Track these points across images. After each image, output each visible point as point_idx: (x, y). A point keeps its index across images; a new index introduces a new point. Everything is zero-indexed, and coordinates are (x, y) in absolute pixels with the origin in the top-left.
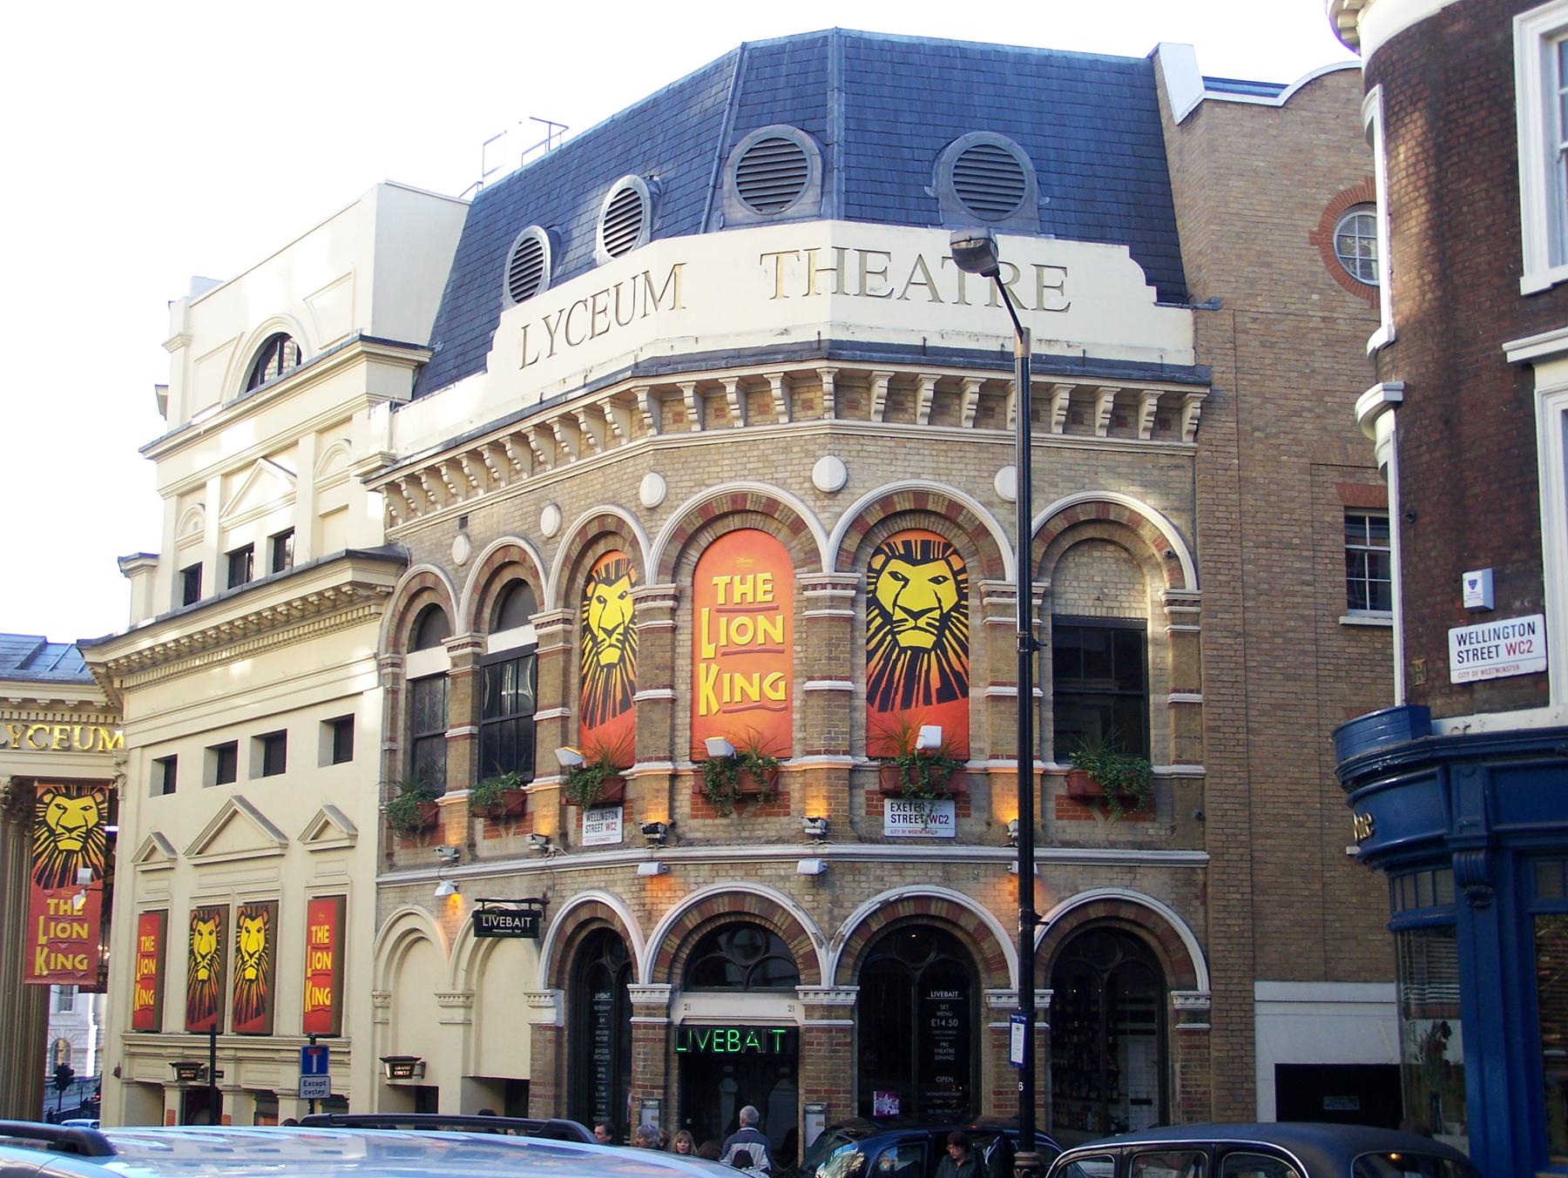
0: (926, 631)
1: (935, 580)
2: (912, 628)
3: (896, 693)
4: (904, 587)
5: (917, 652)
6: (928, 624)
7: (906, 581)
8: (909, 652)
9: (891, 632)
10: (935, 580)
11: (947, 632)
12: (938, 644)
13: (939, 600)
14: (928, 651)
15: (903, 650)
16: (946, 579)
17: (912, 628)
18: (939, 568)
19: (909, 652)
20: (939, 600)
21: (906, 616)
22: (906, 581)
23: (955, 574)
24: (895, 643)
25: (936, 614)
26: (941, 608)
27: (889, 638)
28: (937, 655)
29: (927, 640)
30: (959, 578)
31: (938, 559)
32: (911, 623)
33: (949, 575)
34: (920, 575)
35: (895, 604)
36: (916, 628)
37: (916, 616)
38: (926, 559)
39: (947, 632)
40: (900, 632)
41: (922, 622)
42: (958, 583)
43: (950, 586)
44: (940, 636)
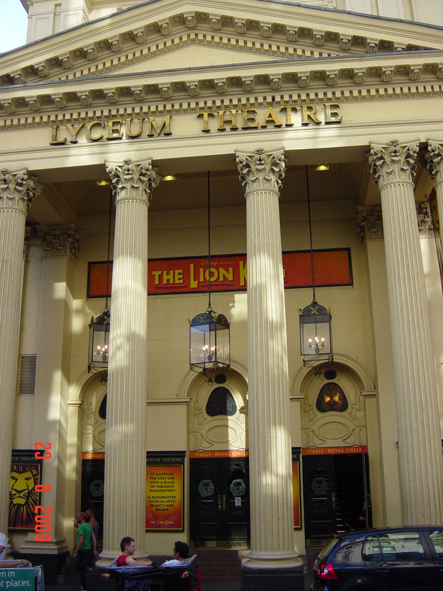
1: (27, 479)
2: (18, 497)
4: (16, 482)
5: (19, 505)
6: (24, 495)
7: (17, 479)
8: (16, 506)
10: (27, 479)
11: (30, 498)
12: (27, 503)
13: (28, 486)
15: (14, 505)
16: (30, 478)
17: (18, 497)
18: (28, 474)
19: (16, 506)
20: (28, 486)
21: (16, 493)
22: (17, 479)
23: (34, 476)
26: (28, 489)
28: (26, 506)
29: (22, 501)
30: (36, 478)
31: (28, 471)
32: (18, 495)
33: (31, 476)
35: (12, 488)
36: (19, 497)
37: (19, 492)
38: (24, 472)
39: (30, 498)
41: (21, 495)
42: (35, 479)
43: (32, 480)
44: (27, 499)
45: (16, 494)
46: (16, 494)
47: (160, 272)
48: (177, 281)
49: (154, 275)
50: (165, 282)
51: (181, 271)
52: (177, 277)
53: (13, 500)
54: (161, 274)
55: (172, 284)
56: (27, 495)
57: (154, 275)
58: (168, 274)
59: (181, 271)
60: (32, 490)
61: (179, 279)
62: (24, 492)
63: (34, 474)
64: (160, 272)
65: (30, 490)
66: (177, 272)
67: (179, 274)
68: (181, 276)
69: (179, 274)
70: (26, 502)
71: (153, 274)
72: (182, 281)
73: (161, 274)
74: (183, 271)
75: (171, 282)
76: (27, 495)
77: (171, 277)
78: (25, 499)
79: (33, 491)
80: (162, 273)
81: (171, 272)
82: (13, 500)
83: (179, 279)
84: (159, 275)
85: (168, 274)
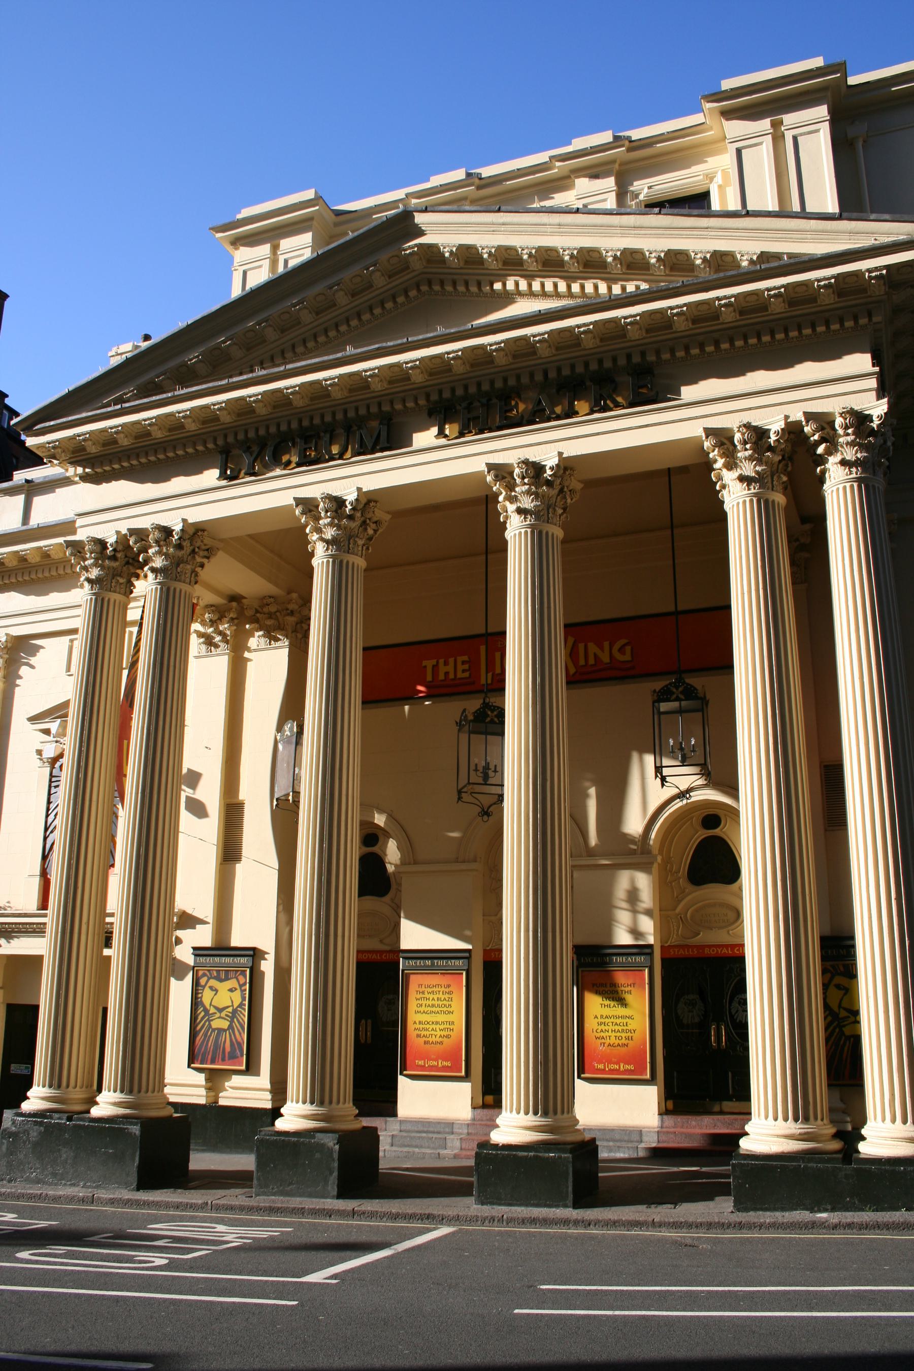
0: (225, 1019)
1: (231, 990)
3: (209, 1054)
5: (220, 1030)
6: (226, 1015)
8: (216, 1031)
9: (208, 1020)
10: (231, 990)
13: (232, 1002)
14: (225, 1030)
15: (214, 1030)
16: (236, 989)
19: (216, 1031)
20: (232, 1002)
21: (216, 1011)
23: (241, 986)
24: (210, 1025)
25: (230, 1009)
26: (233, 1006)
27: (207, 1023)
29: (224, 1024)
30: (243, 988)
32: (218, 1015)
33: (238, 987)
34: (223, 987)
36: (220, 1017)
37: (220, 1010)
39: (235, 1020)
40: (212, 1020)
41: (223, 1014)
43: (238, 992)
44: (232, 1022)
45: (215, 1013)
46: (215, 1013)
47: (434, 662)
48: (460, 675)
49: (425, 667)
50: (442, 677)
51: (465, 658)
52: (460, 667)
53: (211, 1022)
54: (435, 663)
55: (452, 680)
56: (231, 1015)
57: (425, 667)
58: (446, 664)
59: (465, 658)
60: (238, 1007)
61: (464, 671)
62: (227, 1010)
63: (241, 983)
64: (434, 662)
65: (235, 1007)
66: (460, 659)
67: (463, 663)
68: (466, 667)
69: (463, 663)
70: (229, 1026)
71: (424, 665)
72: (467, 674)
73: (435, 663)
74: (469, 658)
75: (452, 676)
76: (231, 1015)
77: (450, 668)
78: (228, 1020)
79: (239, 1009)
80: (438, 662)
81: (451, 660)
82: (211, 1022)
83: (464, 671)
84: (433, 666)
85: (446, 664)
